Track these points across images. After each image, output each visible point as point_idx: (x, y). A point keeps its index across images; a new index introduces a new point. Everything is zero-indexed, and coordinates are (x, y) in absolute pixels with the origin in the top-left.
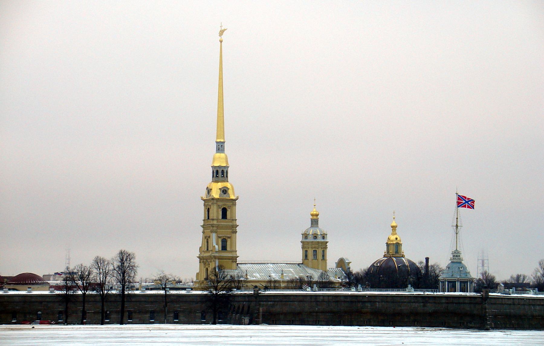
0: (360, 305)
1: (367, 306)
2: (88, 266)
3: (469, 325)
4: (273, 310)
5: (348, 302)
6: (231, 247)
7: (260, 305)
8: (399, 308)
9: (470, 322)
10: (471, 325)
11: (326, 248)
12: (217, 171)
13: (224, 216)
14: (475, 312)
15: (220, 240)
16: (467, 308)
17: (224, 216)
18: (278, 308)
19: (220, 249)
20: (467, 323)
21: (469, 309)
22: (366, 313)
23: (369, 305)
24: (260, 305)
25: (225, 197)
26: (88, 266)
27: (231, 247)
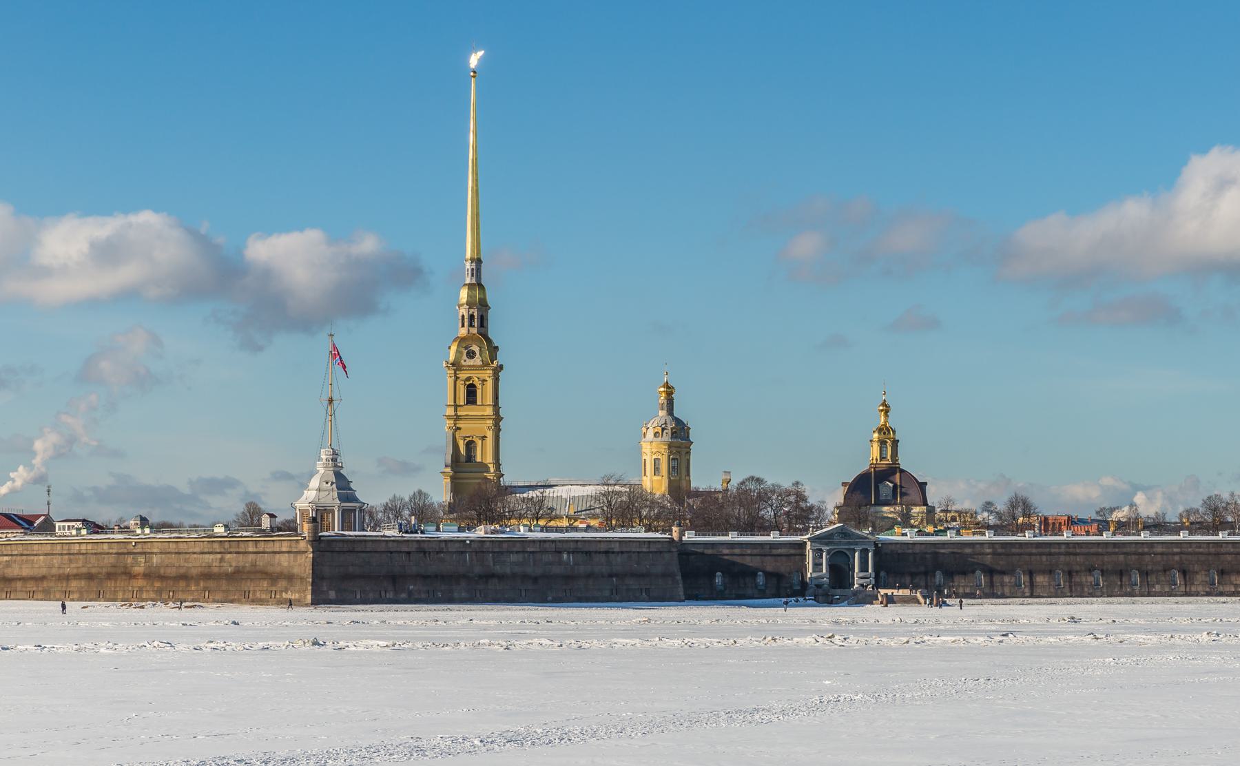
0: (130, 559)
21: (285, 564)
23: (141, 559)
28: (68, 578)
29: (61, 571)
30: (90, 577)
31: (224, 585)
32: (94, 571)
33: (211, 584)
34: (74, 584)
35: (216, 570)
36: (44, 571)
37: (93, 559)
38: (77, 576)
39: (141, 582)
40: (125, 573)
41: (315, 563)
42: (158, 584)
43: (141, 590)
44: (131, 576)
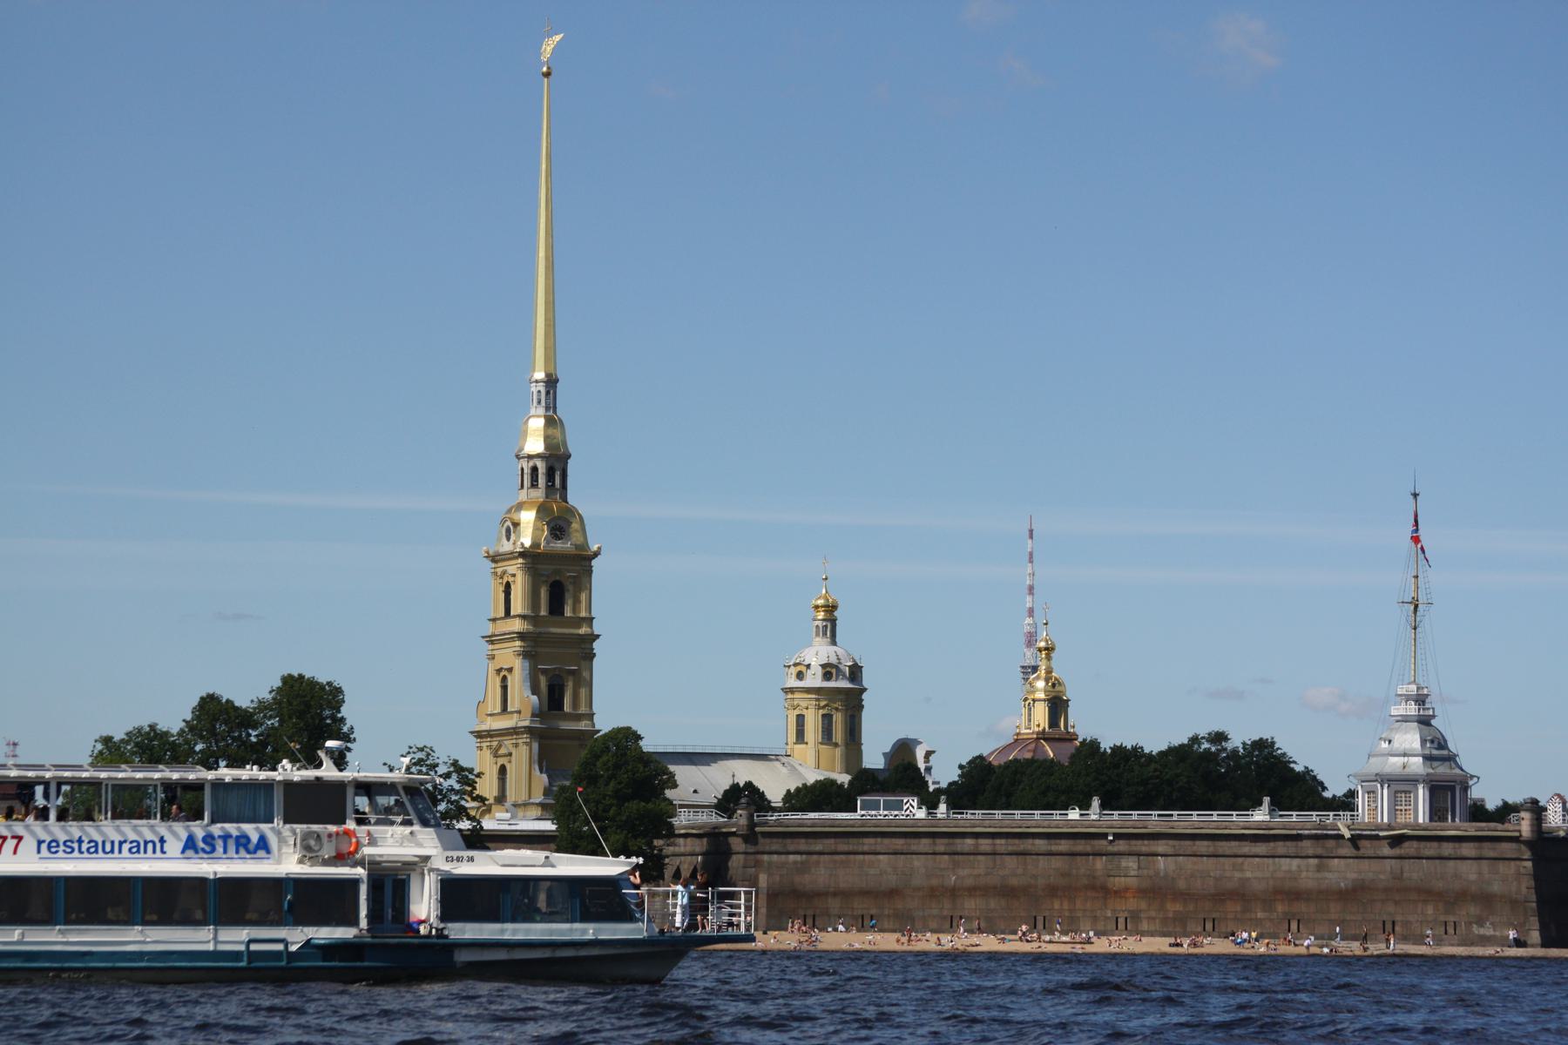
0: (1100, 864)
1: (1127, 868)
2: (175, 731)
3: (1476, 930)
4: (806, 881)
5: (1061, 854)
6: (575, 704)
7: (757, 864)
8: (1238, 875)
9: (1480, 922)
10: (1482, 931)
11: (859, 707)
12: (535, 469)
13: (556, 606)
14: (1496, 888)
15: (543, 681)
16: (1469, 872)
17: (556, 606)
18: (821, 875)
19: (546, 708)
20: (1469, 924)
21: (1473, 877)
22: (1119, 893)
23: (1131, 863)
24: (757, 864)
25: (559, 546)
26: (175, 731)
27: (575, 704)
28: (954, 893)
29: (935, 882)
30: (1008, 892)
31: (1335, 909)
32: (1014, 882)
33: (1302, 908)
34: (970, 905)
35: (1311, 884)
36: (891, 880)
37: (1011, 862)
38: (972, 891)
39: (1132, 904)
40: (1093, 888)
41: (1537, 876)
42: (1173, 908)
43: (1135, 916)
44: (1104, 892)
